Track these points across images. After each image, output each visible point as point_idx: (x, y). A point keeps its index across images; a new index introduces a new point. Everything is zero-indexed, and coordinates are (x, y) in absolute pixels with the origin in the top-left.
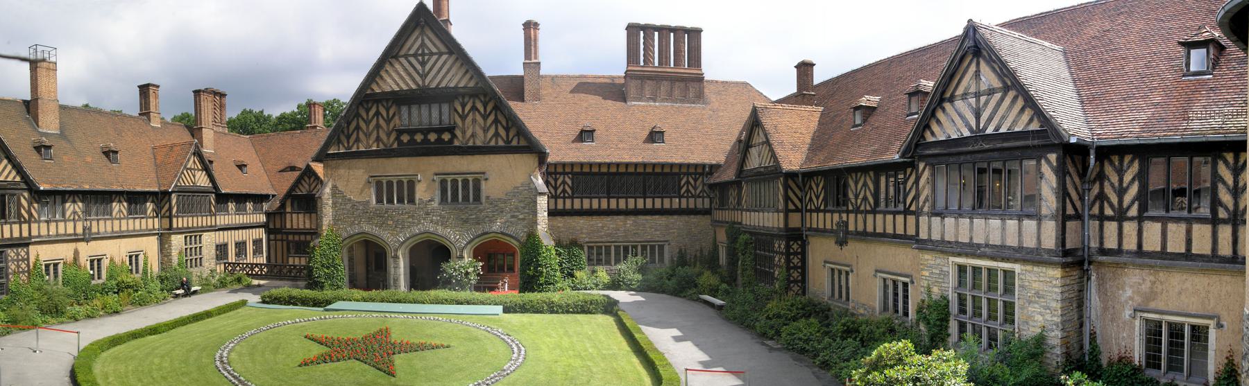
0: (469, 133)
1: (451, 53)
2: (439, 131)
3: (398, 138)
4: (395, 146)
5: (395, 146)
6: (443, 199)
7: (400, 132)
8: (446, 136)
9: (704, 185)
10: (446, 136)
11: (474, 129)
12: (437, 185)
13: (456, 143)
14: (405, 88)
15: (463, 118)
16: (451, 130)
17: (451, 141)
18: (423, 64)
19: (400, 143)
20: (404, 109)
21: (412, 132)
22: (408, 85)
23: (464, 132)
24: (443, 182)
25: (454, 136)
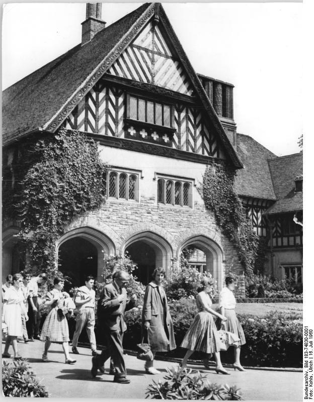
0: (183, 139)
1: (175, 58)
2: (162, 131)
3: (125, 129)
4: (122, 136)
5: (122, 136)
6: (160, 199)
7: (128, 123)
8: (166, 139)
9: (263, 216)
10: (166, 139)
11: (187, 134)
12: (156, 183)
13: (174, 147)
14: (137, 79)
15: (179, 124)
16: (170, 132)
17: (169, 144)
18: (153, 61)
19: (128, 135)
20: (133, 101)
21: (138, 126)
22: (140, 78)
23: (179, 138)
24: (160, 183)
25: (172, 139)
